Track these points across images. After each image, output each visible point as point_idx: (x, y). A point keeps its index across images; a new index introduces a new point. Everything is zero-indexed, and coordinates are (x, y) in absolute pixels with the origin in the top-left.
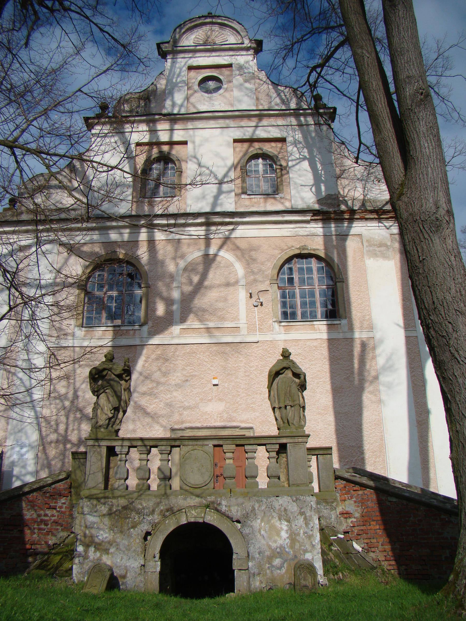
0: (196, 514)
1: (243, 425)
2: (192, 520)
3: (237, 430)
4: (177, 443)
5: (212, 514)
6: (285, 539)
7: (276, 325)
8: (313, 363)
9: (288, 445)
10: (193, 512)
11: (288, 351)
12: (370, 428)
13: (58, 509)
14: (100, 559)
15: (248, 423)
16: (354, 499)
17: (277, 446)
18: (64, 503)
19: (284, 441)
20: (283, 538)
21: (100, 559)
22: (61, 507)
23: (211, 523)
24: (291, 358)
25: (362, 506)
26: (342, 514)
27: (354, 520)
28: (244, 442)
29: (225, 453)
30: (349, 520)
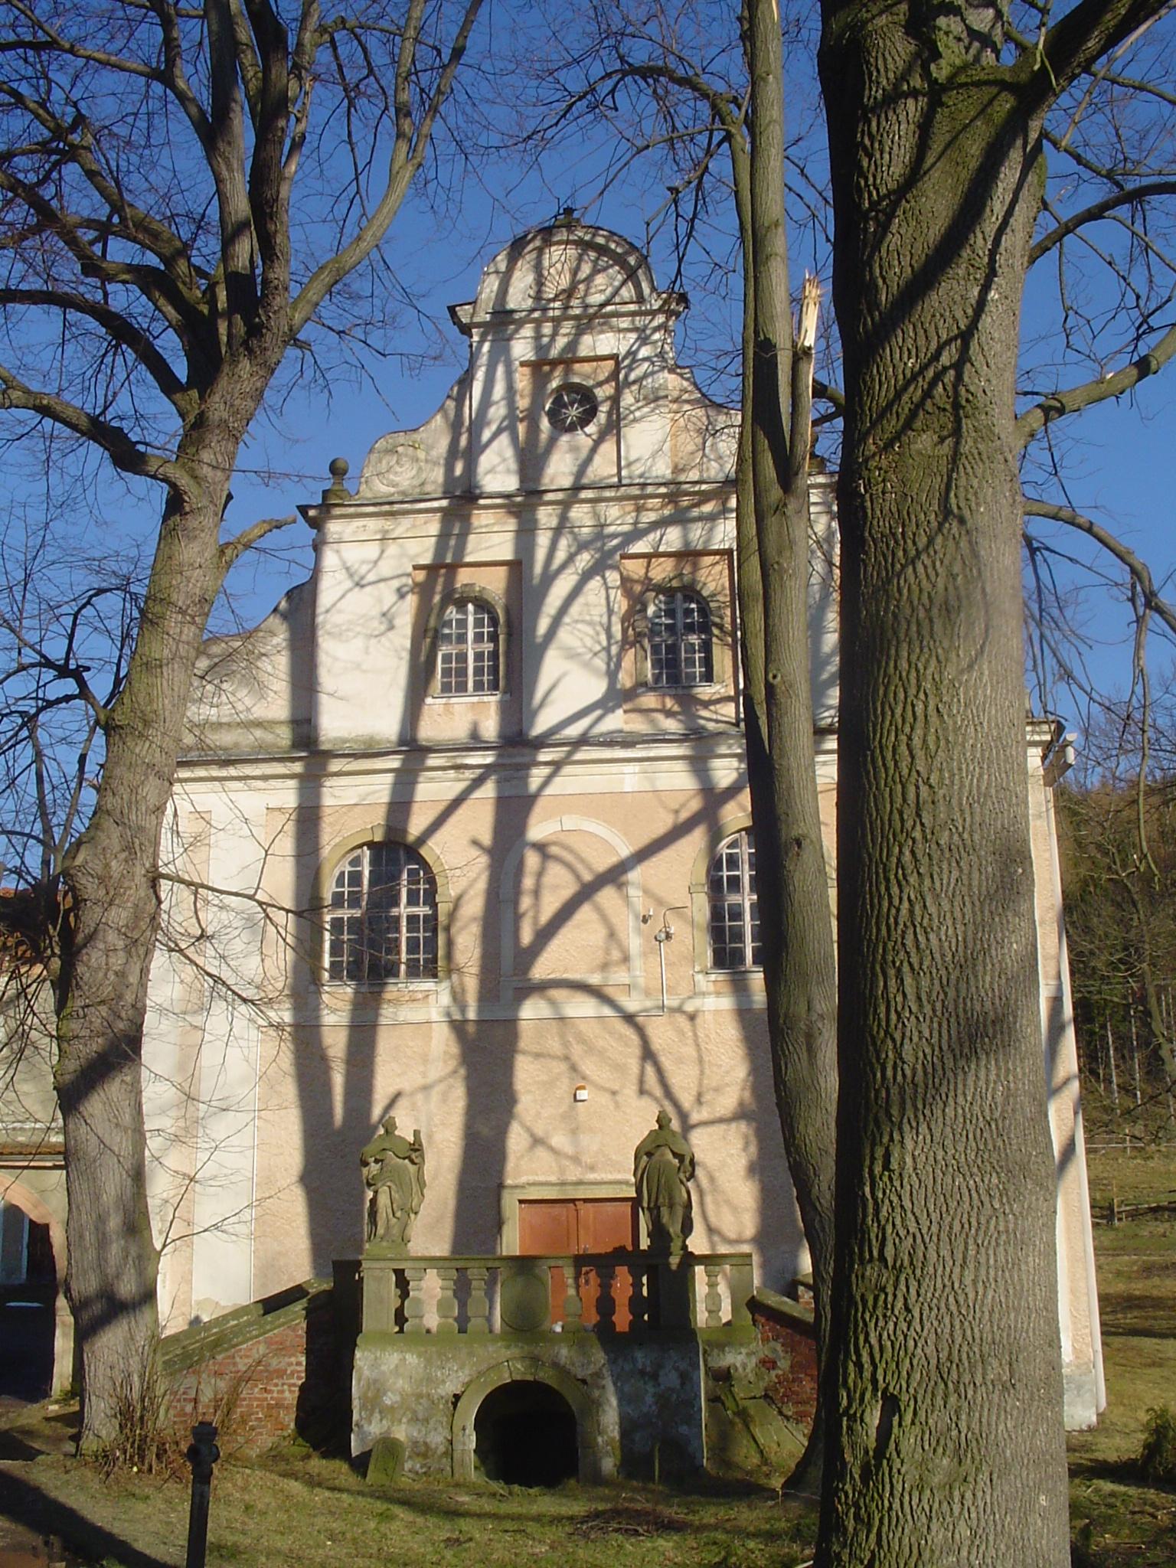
2: (519, 1378)
3: (624, 1187)
7: (699, 977)
30: (773, 1373)
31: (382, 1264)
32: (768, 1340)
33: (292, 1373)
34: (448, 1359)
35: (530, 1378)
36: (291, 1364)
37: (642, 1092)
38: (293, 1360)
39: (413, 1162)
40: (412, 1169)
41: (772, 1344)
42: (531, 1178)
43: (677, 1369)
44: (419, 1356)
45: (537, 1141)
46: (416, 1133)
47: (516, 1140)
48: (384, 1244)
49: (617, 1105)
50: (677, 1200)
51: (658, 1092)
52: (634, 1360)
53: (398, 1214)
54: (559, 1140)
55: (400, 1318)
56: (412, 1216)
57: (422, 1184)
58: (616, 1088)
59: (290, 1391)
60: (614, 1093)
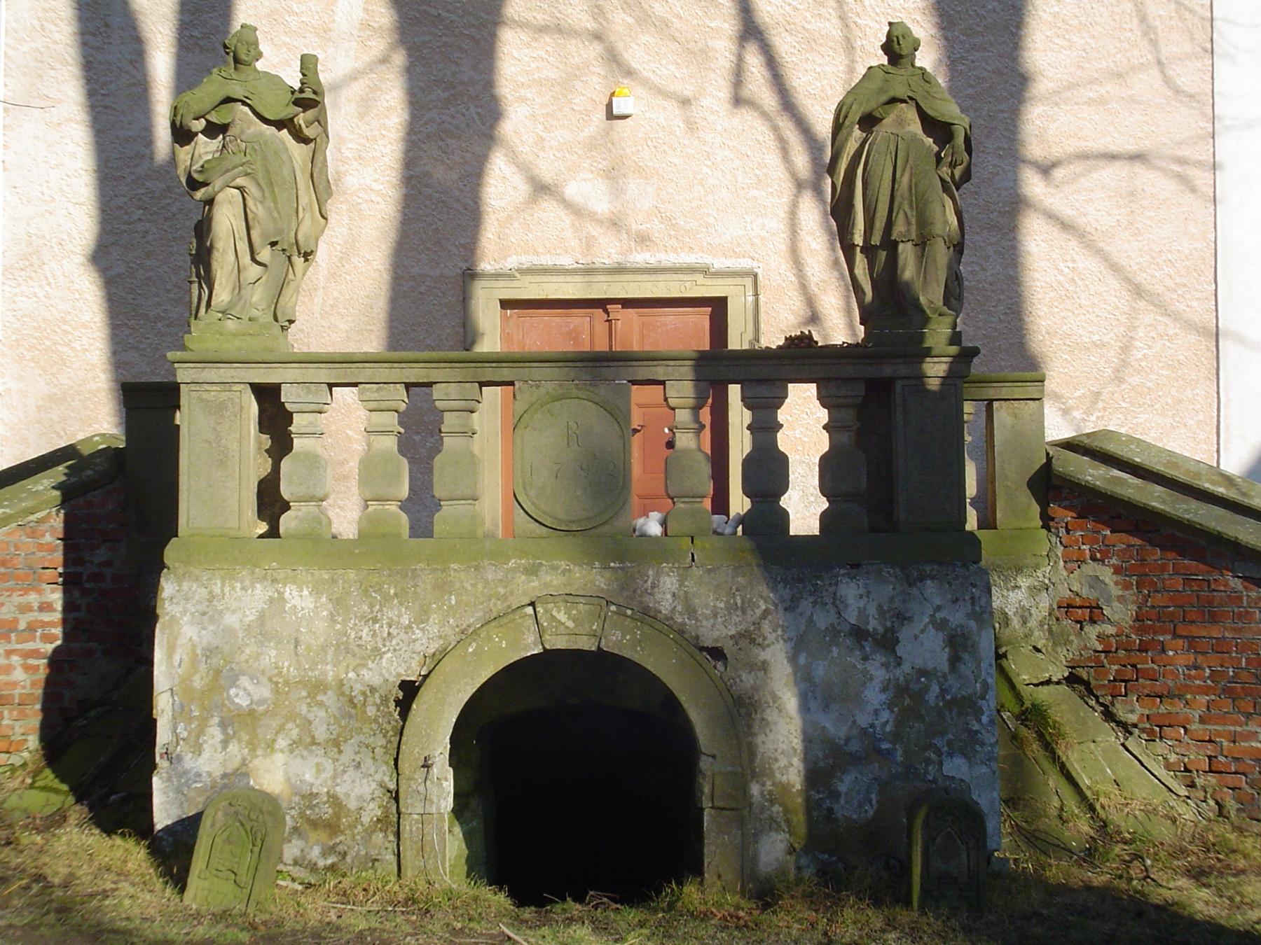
0: (570, 624)
1: (719, 263)
2: (560, 643)
3: (699, 278)
4: (505, 373)
5: (628, 622)
6: (876, 712)
8: (978, 40)
9: (899, 384)
10: (562, 617)
11: (907, 33)
12: (1169, 283)
13: (88, 585)
14: (241, 773)
15: (737, 255)
16: (1114, 561)
17: (860, 390)
18: (107, 564)
19: (887, 371)
20: (870, 708)
21: (241, 773)
22: (97, 577)
23: (627, 654)
24: (918, 64)
25: (1139, 586)
26: (1068, 607)
27: (1110, 630)
28: (745, 373)
29: (673, 409)
30: (1092, 631)
31: (225, 373)
32: (1081, 561)
33: (31, 628)
34: (387, 599)
35: (587, 644)
36: (26, 608)
37: (738, 100)
38: (33, 598)
39: (301, 138)
40: (298, 152)
41: (1091, 568)
42: (526, 260)
43: (940, 625)
44: (316, 591)
45: (541, 189)
46: (308, 65)
47: (501, 186)
48: (231, 325)
49: (691, 126)
50: (938, 228)
51: (768, 99)
52: (838, 605)
53: (265, 254)
54: (585, 188)
55: (271, 502)
56: (298, 261)
57: (322, 187)
58: (688, 91)
59: (27, 668)
60: (685, 102)
